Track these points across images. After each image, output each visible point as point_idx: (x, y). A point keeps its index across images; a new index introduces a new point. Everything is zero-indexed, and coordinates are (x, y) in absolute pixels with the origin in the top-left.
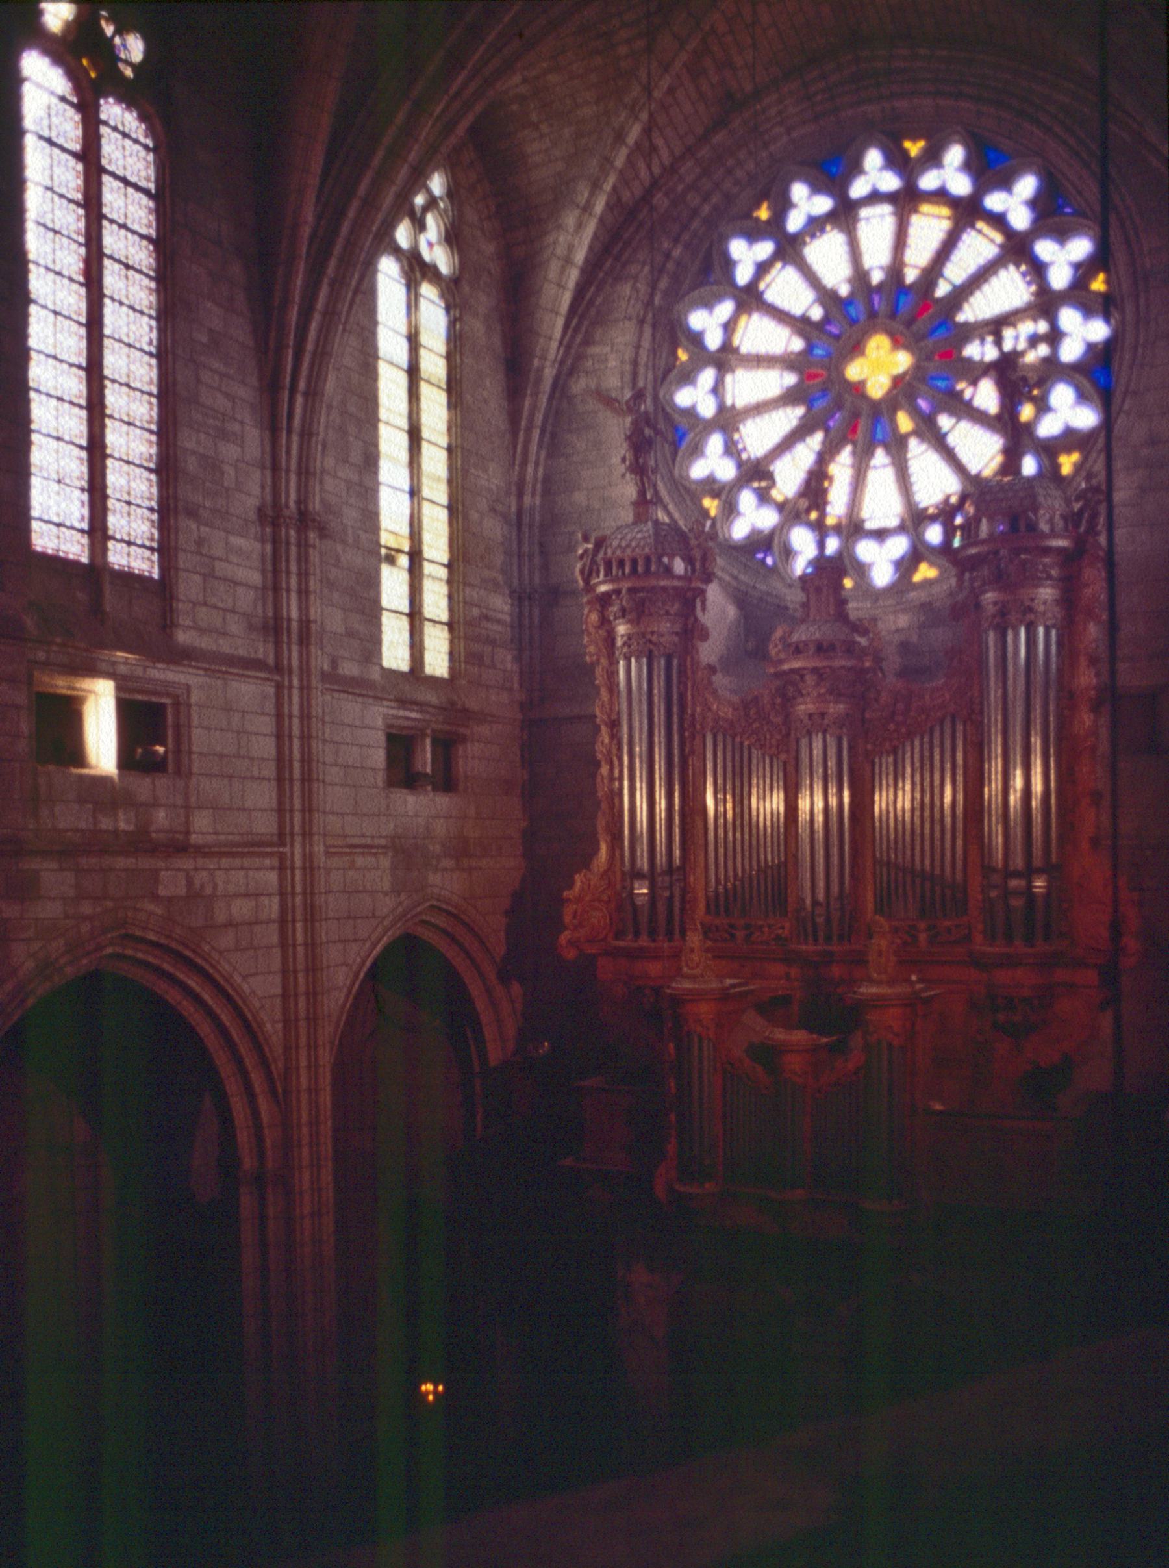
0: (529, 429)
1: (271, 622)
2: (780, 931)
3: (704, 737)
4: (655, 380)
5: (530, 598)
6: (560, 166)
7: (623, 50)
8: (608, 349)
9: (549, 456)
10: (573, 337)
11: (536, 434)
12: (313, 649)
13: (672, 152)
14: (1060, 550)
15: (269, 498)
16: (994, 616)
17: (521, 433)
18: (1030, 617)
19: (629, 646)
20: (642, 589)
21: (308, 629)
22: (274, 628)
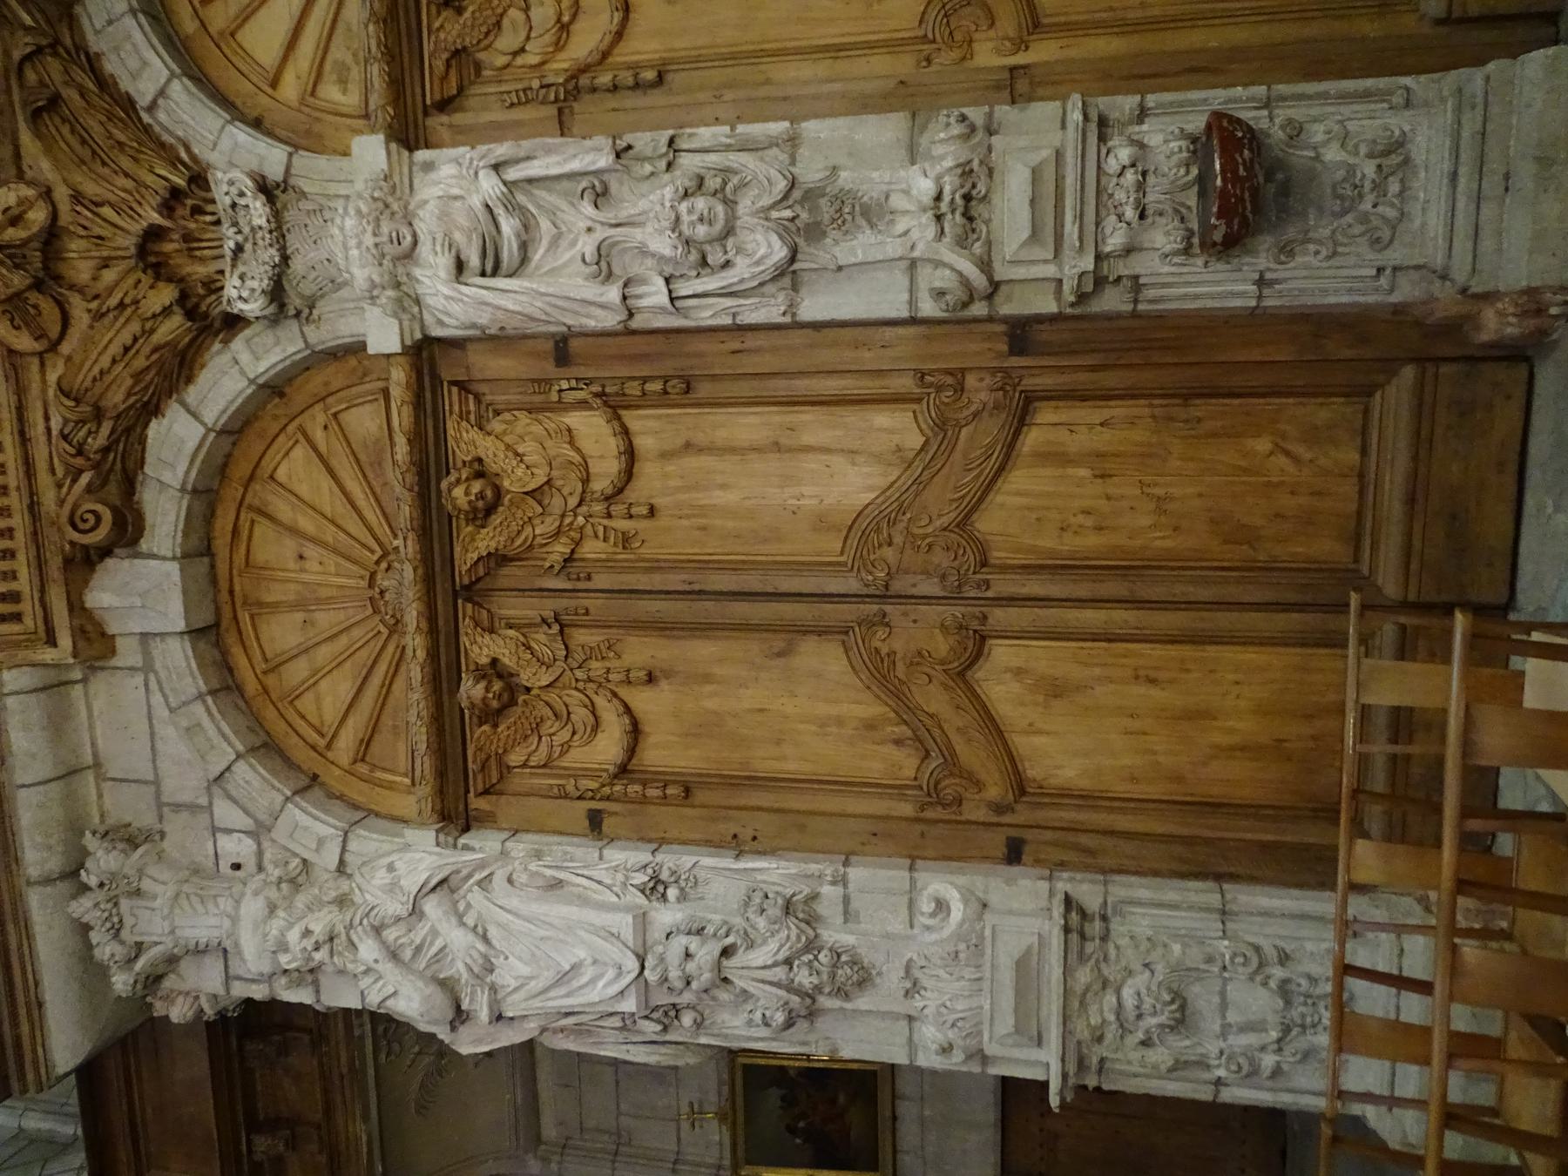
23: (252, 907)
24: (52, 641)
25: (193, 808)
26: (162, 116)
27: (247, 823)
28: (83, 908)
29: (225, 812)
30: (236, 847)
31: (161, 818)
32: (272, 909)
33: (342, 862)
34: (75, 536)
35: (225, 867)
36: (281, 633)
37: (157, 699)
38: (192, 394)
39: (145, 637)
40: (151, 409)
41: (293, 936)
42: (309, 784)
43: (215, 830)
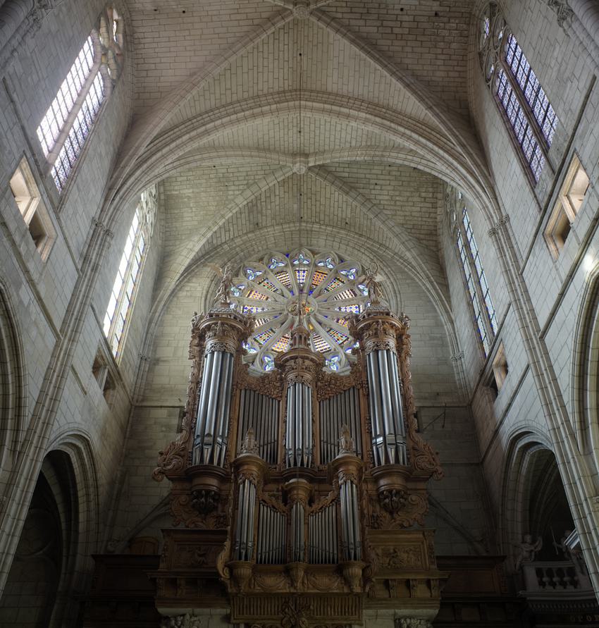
0: (159, 302)
1: (84, 254)
6: (196, 223)
7: (231, 193)
10: (183, 279)
12: (97, 274)
13: (234, 234)
15: (97, 217)
17: (156, 302)
22: (86, 259)
24: (234, 619)
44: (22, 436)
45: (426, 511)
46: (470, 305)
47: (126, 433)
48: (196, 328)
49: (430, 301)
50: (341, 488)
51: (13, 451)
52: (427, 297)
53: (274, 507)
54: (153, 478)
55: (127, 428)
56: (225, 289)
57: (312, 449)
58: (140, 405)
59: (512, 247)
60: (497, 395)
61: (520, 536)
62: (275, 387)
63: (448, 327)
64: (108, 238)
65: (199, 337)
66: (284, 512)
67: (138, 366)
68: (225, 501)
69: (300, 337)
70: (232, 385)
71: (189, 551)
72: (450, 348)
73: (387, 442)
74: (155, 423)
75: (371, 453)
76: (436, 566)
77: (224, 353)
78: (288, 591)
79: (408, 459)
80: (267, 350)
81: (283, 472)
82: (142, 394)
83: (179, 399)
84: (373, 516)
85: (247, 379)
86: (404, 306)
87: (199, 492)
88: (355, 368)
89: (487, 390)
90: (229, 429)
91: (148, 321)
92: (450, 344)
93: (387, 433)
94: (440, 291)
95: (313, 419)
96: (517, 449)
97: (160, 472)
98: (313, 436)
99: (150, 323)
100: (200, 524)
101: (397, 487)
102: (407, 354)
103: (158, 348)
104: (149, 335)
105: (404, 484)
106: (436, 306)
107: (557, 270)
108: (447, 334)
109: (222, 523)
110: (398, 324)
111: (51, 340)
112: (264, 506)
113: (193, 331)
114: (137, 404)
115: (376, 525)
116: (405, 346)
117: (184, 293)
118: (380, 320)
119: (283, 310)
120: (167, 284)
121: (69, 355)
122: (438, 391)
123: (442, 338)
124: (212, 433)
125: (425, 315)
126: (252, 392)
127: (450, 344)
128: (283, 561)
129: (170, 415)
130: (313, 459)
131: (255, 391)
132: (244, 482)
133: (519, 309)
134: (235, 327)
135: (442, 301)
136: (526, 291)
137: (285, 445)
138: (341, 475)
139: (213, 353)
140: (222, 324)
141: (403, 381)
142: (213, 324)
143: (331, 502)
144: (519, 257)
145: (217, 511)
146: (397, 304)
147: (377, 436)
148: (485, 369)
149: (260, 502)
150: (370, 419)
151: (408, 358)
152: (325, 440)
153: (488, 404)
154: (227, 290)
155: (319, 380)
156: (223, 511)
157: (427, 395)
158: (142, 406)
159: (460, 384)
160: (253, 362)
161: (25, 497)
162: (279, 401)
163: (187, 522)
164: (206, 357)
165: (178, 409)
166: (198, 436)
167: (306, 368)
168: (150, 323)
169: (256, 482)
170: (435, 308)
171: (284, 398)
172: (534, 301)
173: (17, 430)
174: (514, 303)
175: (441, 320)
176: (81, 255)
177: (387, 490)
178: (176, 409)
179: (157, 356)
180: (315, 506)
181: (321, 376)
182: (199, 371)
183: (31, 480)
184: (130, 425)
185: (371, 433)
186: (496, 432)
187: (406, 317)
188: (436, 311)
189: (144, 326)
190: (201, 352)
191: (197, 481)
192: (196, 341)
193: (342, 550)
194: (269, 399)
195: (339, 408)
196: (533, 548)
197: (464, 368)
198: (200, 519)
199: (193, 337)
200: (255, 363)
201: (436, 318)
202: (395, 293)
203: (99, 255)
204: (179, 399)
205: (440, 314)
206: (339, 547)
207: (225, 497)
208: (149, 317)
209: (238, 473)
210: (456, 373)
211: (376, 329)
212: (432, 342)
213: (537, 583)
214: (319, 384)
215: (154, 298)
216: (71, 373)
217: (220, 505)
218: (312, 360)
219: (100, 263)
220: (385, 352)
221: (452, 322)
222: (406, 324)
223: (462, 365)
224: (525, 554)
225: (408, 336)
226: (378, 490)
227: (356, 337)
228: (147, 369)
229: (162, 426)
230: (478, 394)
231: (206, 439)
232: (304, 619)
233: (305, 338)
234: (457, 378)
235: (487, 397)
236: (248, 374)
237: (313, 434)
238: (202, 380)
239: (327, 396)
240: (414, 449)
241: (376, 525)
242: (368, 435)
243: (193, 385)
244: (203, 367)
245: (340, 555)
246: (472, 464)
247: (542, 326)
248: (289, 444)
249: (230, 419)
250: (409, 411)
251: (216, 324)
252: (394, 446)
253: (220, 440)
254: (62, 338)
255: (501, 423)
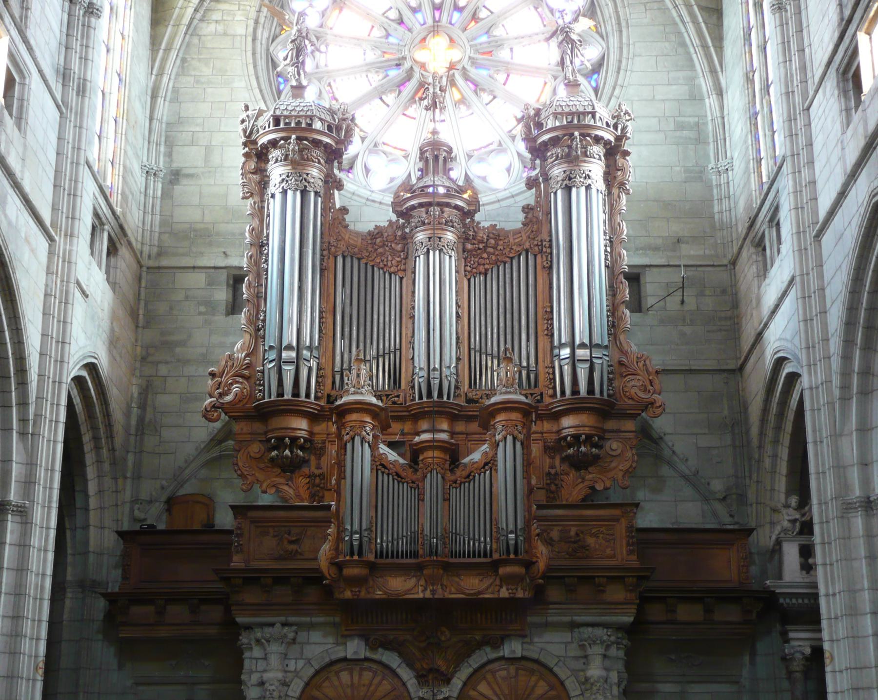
0: (168, 50)
1: (62, 69)
2: (396, 399)
3: (336, 257)
4: (268, 39)
5: (155, 174)
8: (236, 7)
9: (177, 75)
11: (173, 54)
14: (607, 143)
16: (563, 180)
17: (161, 52)
18: (589, 182)
19: (287, 181)
20: (306, 139)
21: (84, 86)
22: (65, 75)
23: (280, 675)
24: (346, 630)
25: (302, 653)
26: (466, 664)
27: (298, 670)
28: (278, 625)
29: (301, 663)
30: (292, 667)
31: (299, 643)
32: (279, 681)
33: (289, 696)
34: (371, 639)
35: (287, 662)
36: (345, 676)
37: (330, 646)
38: (404, 665)
39: (345, 644)
40: (401, 655)
41: (273, 687)
42: (307, 684)
43: (296, 659)
44: (32, 409)
45: (631, 466)
46: (749, 80)
47: (138, 317)
48: (249, 141)
49: (683, 44)
50: (498, 445)
51: (23, 434)
52: (680, 33)
53: (397, 475)
54: (204, 416)
55: (138, 309)
56: (298, 56)
57: (456, 367)
58: (156, 265)
59: (802, 50)
60: (765, 276)
61: (782, 497)
62: (394, 252)
63: (711, 102)
64: (93, 20)
65: (256, 155)
66: (413, 482)
67: (143, 190)
68: (320, 452)
69: (436, 158)
70: (322, 250)
71: (275, 536)
72: (711, 146)
73: (577, 358)
74: (187, 298)
75: (551, 371)
76: (635, 557)
77: (304, 192)
78: (421, 596)
79: (610, 380)
80: (375, 145)
81: (410, 406)
82: (156, 243)
83: (224, 253)
84: (549, 474)
85: (347, 238)
86: (634, 56)
87: (281, 439)
88: (530, 216)
89: (757, 254)
90: (320, 331)
91: (149, 93)
92: (711, 140)
93: (577, 342)
94: (703, 25)
95: (457, 313)
96: (784, 375)
97: (214, 406)
98: (457, 343)
99: (154, 97)
100: (286, 488)
101: (587, 430)
102: (622, 185)
103: (175, 149)
104: (155, 123)
105: (600, 425)
106: (694, 56)
107: (843, 149)
108: (709, 118)
109: (318, 486)
110: (608, 136)
111: (43, 244)
112: (383, 473)
113: (245, 144)
114: (151, 263)
115: (553, 487)
116: (619, 173)
117: (212, 27)
118: (576, 133)
119: (404, 58)
120: (177, 10)
121: (69, 262)
122: (681, 234)
123: (699, 127)
124: (294, 344)
125: (672, 75)
126: (354, 259)
127: (711, 140)
128: (415, 555)
129: (210, 283)
130: (457, 381)
131: (359, 259)
132: (353, 439)
133: (797, 172)
134: (320, 141)
135: (705, 46)
136: (810, 145)
137: (413, 358)
138: (500, 428)
139: (284, 192)
140: (299, 139)
141: (611, 242)
142: (282, 138)
143: (484, 467)
144: (809, 75)
145: (309, 467)
146: (621, 48)
147: (561, 346)
148: (757, 215)
149: (380, 465)
150: (552, 312)
151: (624, 197)
152: (478, 348)
153: (756, 279)
154: (301, 59)
155: (467, 239)
156: (318, 467)
157: (659, 241)
158: (159, 268)
159: (721, 220)
160: (351, 168)
161: (50, 497)
162: (401, 279)
163: (265, 485)
164: (273, 196)
165: (225, 271)
166: (271, 347)
167: (447, 222)
168: (154, 97)
169: (370, 438)
170: (691, 60)
171: (409, 272)
172: (818, 166)
173: (23, 404)
174: (789, 159)
175: (700, 87)
176: (57, 71)
177: (572, 436)
178: (220, 270)
179: (175, 165)
180: (459, 473)
181: (471, 233)
182: (261, 221)
183: (53, 470)
184: (142, 303)
185: (552, 335)
186: (759, 336)
187: (626, 113)
188: (692, 67)
189: (144, 108)
190: (264, 184)
191: (278, 422)
192: (252, 165)
193: (498, 539)
194: (385, 273)
195: (502, 291)
196: (798, 516)
197: (731, 193)
198: (282, 480)
199: (246, 155)
200: (355, 170)
201: (691, 81)
202: (619, 24)
203: (85, 59)
204: (224, 253)
205: (701, 75)
206: (494, 534)
207: (320, 445)
208: (151, 85)
209: (343, 424)
210: (716, 198)
211: (570, 147)
212: (678, 134)
213: (798, 567)
214: (469, 246)
215: (155, 41)
216: (78, 294)
217: (313, 458)
218: (457, 207)
219: (89, 78)
220: (583, 189)
221: (720, 93)
222: (624, 128)
223: (728, 183)
224: (786, 524)
225: (626, 153)
226: (559, 432)
227: (535, 154)
228: (159, 193)
229: (199, 304)
230: (745, 254)
231: (284, 354)
232: (443, 629)
233: (444, 157)
234: (716, 209)
235: (754, 267)
236: (346, 226)
237: (458, 338)
238: (268, 240)
239: (482, 269)
240: (621, 363)
241: (553, 487)
242: (547, 340)
243: (253, 251)
244: (268, 216)
245: (494, 546)
246: (724, 371)
247: (822, 214)
248: (420, 361)
249: (321, 312)
250: (619, 297)
251: (286, 139)
252: (587, 365)
253: (309, 354)
254: (57, 238)
255: (766, 325)
